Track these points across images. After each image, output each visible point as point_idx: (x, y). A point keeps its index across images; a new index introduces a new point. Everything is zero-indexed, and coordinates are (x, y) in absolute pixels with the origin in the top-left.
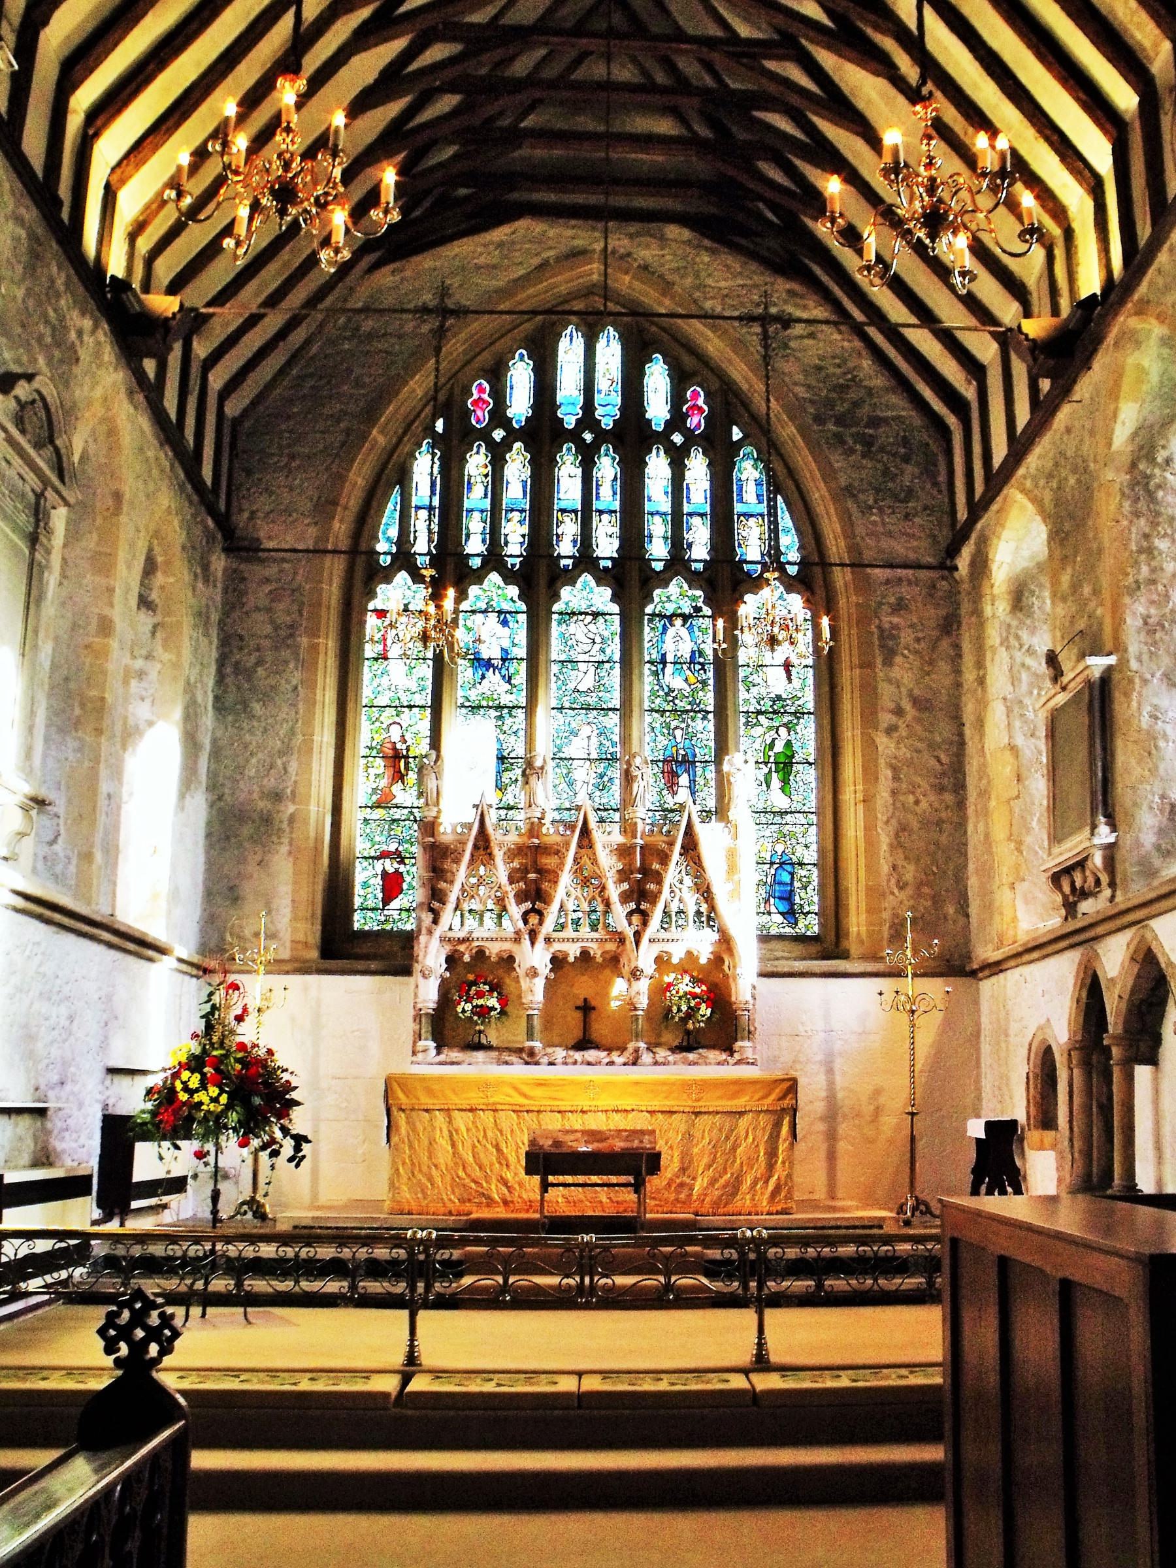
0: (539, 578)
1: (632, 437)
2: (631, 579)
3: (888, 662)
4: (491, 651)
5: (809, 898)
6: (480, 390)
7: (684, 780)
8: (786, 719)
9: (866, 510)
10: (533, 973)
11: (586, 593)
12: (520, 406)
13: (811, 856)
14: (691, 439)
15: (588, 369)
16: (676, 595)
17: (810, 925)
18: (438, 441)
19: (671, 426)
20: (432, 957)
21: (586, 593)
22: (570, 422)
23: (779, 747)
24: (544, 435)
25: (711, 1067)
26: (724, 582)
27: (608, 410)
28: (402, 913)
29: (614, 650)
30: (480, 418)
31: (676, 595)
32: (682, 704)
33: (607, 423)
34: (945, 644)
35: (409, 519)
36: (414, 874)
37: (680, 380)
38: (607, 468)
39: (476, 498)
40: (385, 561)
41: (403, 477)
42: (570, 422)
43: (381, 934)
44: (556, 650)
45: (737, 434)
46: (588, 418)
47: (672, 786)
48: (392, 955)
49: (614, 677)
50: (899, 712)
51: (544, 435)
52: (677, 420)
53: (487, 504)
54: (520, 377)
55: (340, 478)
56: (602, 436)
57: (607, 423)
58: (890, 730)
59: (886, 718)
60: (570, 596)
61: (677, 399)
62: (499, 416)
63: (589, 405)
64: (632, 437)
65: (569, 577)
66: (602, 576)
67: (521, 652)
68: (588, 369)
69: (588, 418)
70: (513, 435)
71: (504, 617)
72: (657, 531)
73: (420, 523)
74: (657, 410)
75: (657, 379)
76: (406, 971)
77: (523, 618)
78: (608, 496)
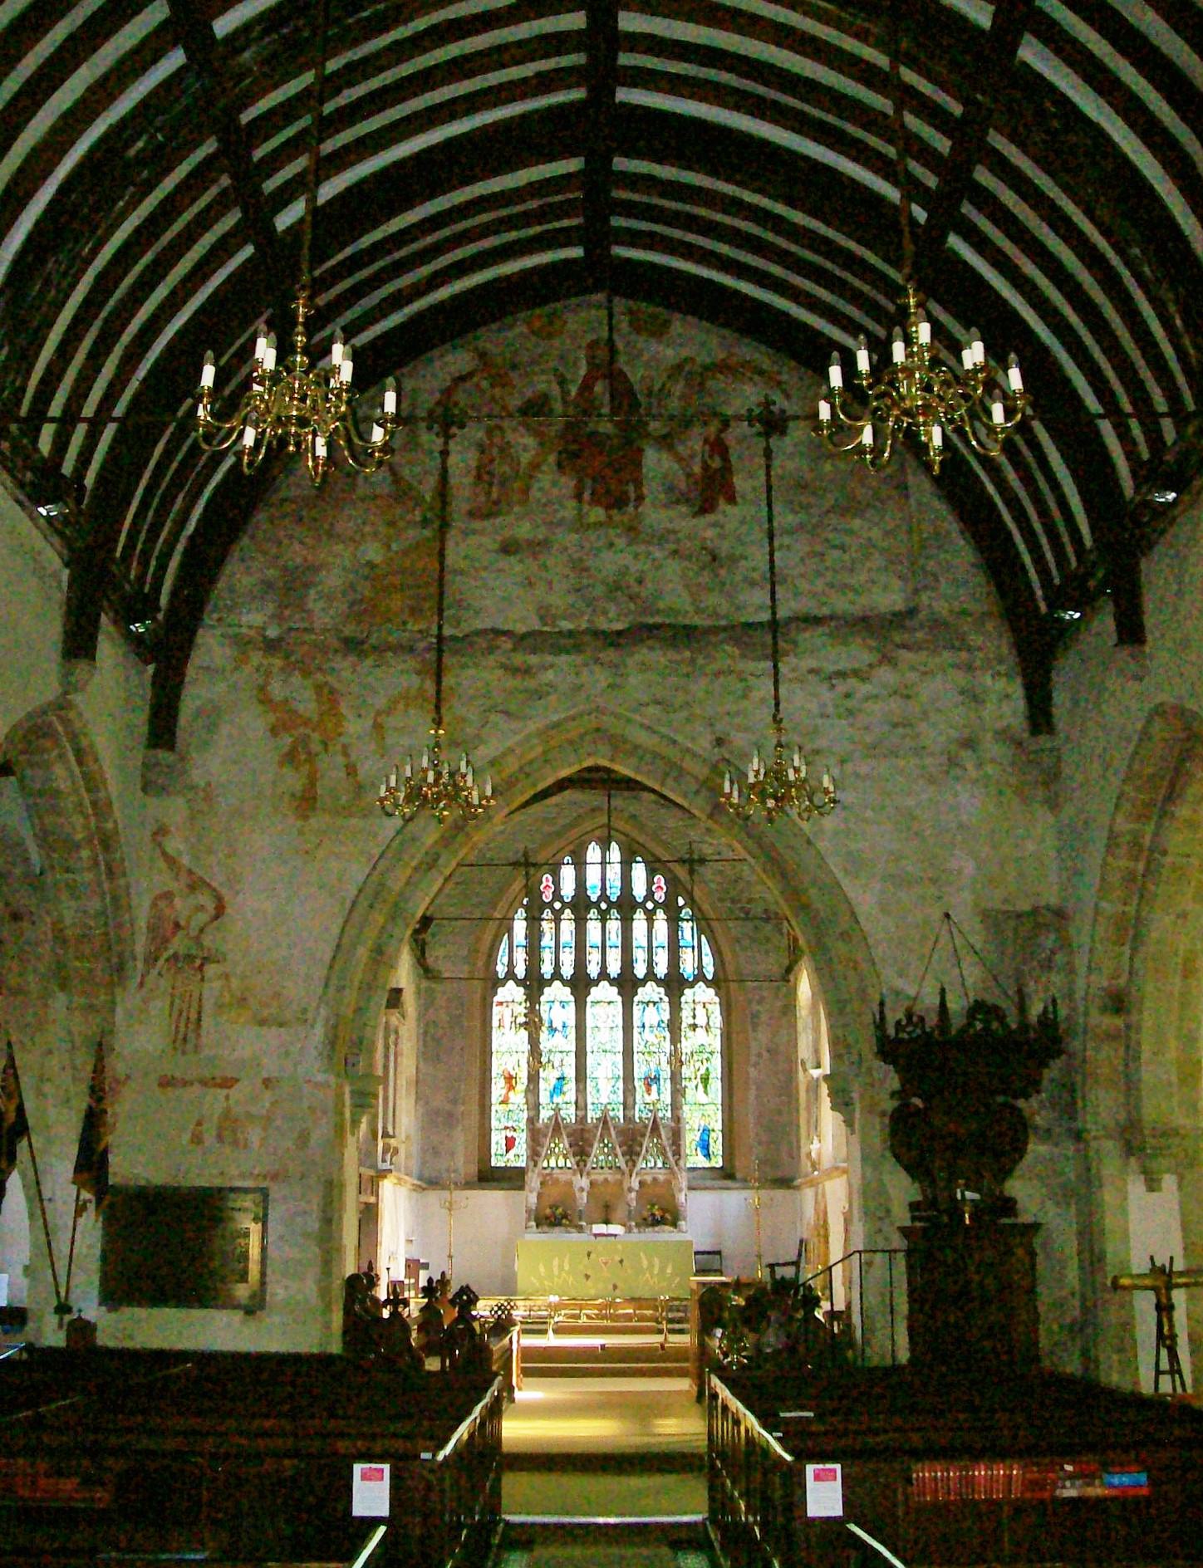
0: (580, 984)
1: (626, 906)
2: (627, 984)
3: (754, 1030)
4: (557, 1024)
5: (717, 1148)
6: (547, 879)
7: (654, 1087)
8: (706, 1056)
9: (744, 949)
10: (582, 1189)
11: (605, 992)
12: (568, 889)
13: (718, 1126)
14: (657, 905)
15: (603, 868)
16: (650, 991)
17: (717, 1162)
18: (527, 908)
19: (646, 899)
20: (533, 1180)
21: (605, 992)
22: (594, 898)
23: (703, 1071)
24: (581, 905)
25: (666, 1234)
26: (675, 984)
27: (614, 893)
28: (518, 1157)
29: (619, 1021)
30: (547, 897)
31: (650, 991)
32: (653, 1049)
33: (614, 898)
34: (784, 1021)
35: (512, 955)
36: (522, 1138)
37: (651, 873)
38: (614, 926)
39: (547, 941)
40: (501, 975)
41: (510, 930)
42: (594, 898)
43: (506, 1168)
44: (590, 1022)
45: (681, 902)
46: (604, 897)
47: (649, 1091)
48: (511, 1178)
49: (619, 1034)
50: (759, 1055)
51: (581, 905)
52: (650, 895)
53: (553, 944)
54: (568, 873)
55: (478, 939)
56: (611, 905)
57: (614, 898)
58: (755, 1065)
59: (753, 1059)
60: (596, 993)
61: (650, 883)
62: (557, 895)
63: (603, 888)
64: (626, 906)
65: (596, 983)
66: (612, 982)
67: (572, 1022)
68: (603, 868)
69: (604, 897)
70: (565, 905)
71: (563, 1004)
72: (640, 956)
73: (520, 956)
74: (639, 891)
75: (639, 872)
76: (521, 1188)
77: (573, 1005)
78: (614, 938)
